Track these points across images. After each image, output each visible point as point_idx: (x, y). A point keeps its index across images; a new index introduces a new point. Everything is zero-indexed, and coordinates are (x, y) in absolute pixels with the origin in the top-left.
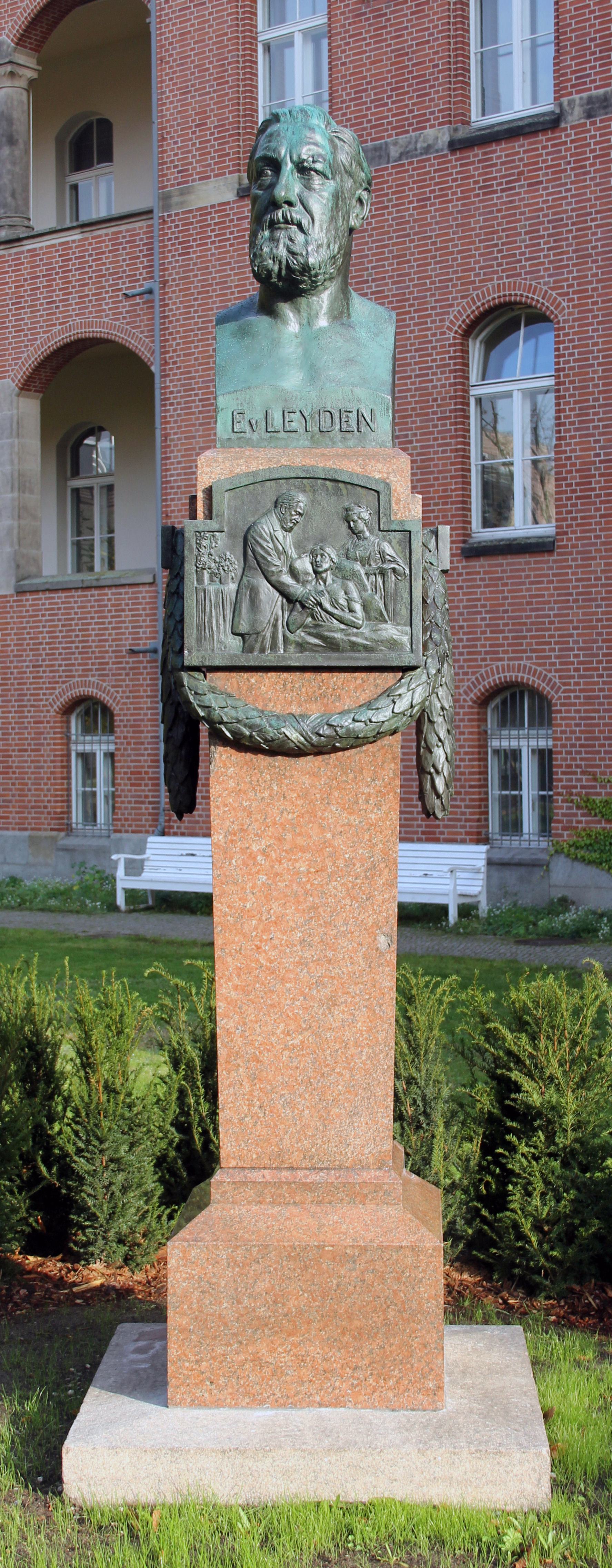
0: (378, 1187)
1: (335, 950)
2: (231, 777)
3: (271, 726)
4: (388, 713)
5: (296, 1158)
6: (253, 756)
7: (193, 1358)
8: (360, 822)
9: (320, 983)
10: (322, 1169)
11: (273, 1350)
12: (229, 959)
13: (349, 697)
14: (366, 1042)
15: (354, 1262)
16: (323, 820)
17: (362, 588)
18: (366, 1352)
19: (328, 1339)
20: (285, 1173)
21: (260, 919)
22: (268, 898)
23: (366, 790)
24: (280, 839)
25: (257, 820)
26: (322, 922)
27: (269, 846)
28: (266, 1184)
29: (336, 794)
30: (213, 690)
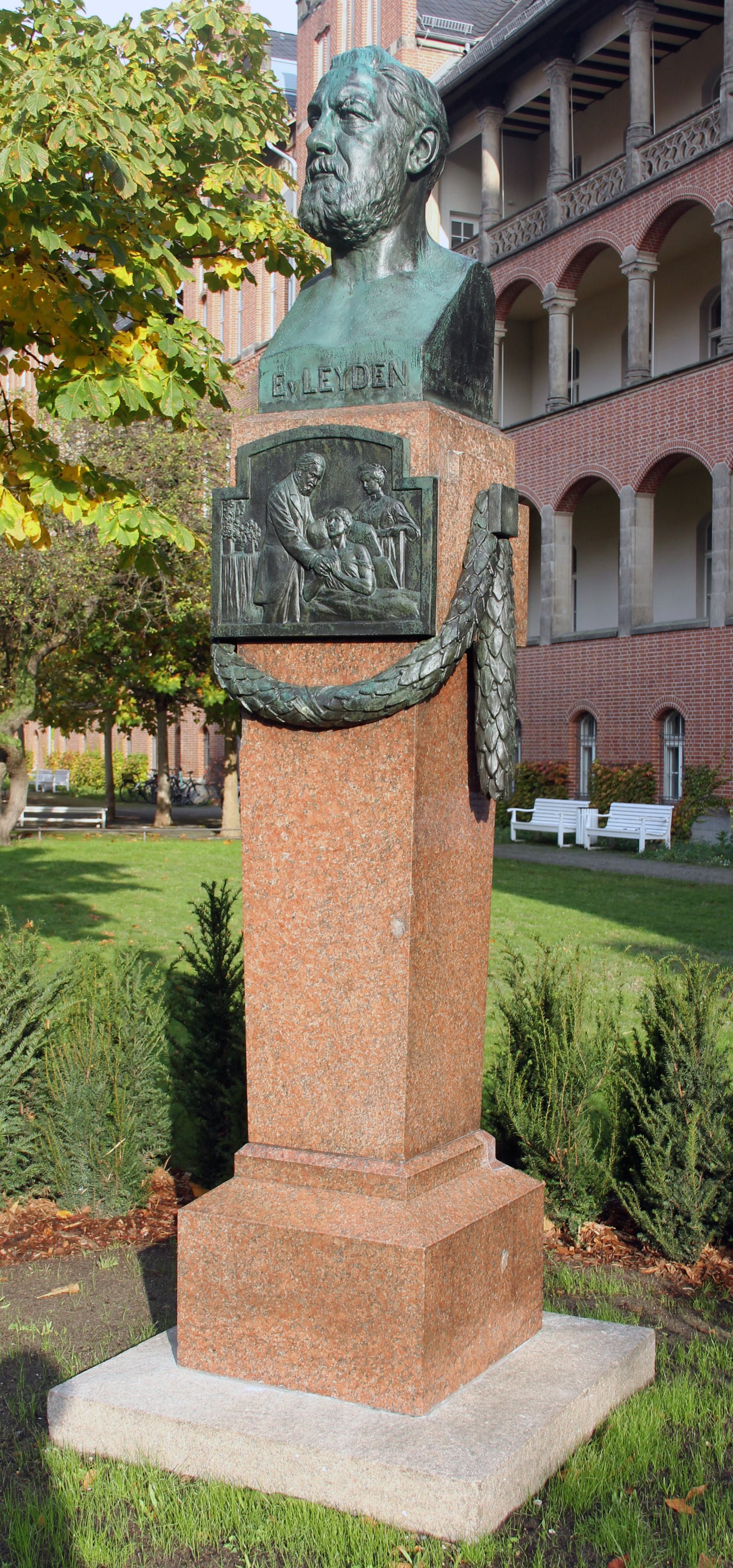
0: (384, 1180)
1: (351, 933)
2: (258, 751)
3: (282, 698)
4: (395, 687)
5: (314, 1140)
6: (278, 730)
7: (198, 1324)
8: (376, 801)
9: (337, 966)
10: (337, 1155)
11: (267, 1329)
12: (256, 936)
13: (367, 668)
14: (379, 1030)
15: (341, 1254)
16: (342, 797)
17: (374, 553)
18: (350, 1346)
19: (316, 1326)
20: (303, 1155)
21: (283, 897)
22: (291, 875)
23: (382, 767)
24: (302, 816)
25: (281, 796)
26: (339, 903)
27: (292, 823)
28: (283, 1164)
29: (354, 771)
30: (236, 662)
